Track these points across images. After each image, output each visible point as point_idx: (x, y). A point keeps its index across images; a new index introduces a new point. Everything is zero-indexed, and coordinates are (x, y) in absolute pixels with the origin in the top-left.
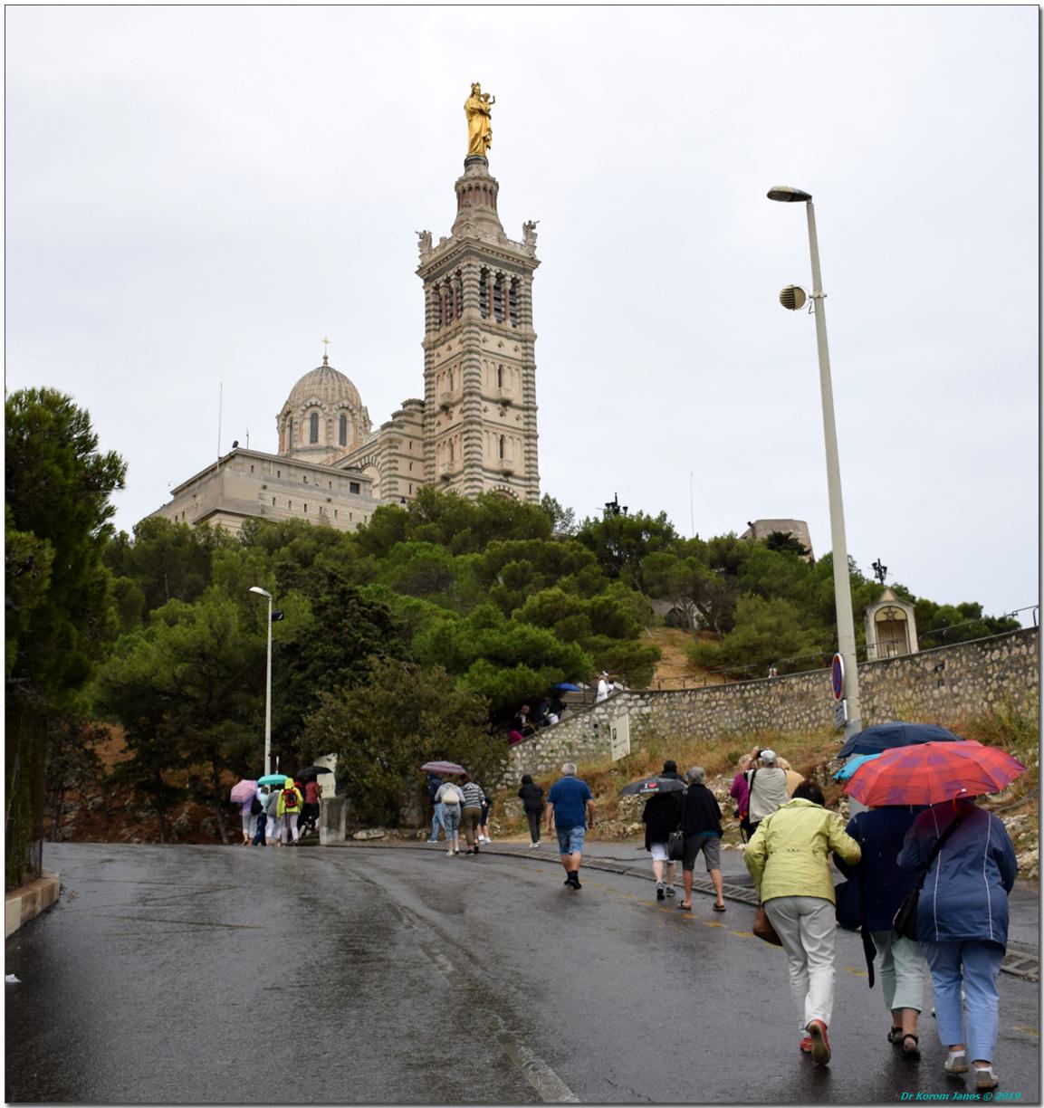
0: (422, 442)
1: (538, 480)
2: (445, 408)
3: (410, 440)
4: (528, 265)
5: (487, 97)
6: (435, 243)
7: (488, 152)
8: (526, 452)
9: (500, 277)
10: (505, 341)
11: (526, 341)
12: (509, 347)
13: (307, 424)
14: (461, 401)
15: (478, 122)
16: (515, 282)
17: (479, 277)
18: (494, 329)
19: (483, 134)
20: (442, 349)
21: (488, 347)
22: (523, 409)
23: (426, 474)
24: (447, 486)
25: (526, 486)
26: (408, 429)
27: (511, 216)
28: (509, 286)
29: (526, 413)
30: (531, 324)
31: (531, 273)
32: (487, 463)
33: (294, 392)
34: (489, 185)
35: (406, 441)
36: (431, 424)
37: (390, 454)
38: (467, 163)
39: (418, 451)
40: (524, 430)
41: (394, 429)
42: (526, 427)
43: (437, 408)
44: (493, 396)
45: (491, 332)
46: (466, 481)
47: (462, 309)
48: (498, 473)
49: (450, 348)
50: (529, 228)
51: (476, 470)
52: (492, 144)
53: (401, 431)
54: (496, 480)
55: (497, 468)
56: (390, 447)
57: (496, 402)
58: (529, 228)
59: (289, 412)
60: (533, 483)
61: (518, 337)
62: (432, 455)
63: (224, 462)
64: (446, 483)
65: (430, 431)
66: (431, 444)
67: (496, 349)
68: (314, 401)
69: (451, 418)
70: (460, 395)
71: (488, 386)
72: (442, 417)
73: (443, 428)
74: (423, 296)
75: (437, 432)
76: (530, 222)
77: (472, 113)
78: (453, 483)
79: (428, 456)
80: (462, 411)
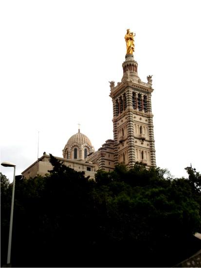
2: (121, 142)
3: (108, 154)
4: (148, 91)
5: (132, 34)
6: (116, 85)
7: (133, 53)
9: (140, 95)
10: (142, 118)
11: (149, 117)
12: (144, 120)
13: (73, 153)
14: (127, 139)
15: (130, 42)
16: (145, 97)
17: (132, 95)
18: (138, 113)
19: (132, 46)
20: (119, 122)
21: (136, 119)
26: (108, 150)
27: (142, 75)
28: (143, 98)
30: (151, 111)
31: (150, 93)
33: (68, 142)
34: (134, 64)
36: (116, 148)
37: (102, 159)
38: (126, 57)
39: (112, 158)
41: (103, 150)
43: (118, 142)
45: (137, 114)
47: (126, 107)
49: (122, 121)
50: (149, 78)
52: (135, 50)
56: (102, 157)
57: (139, 139)
58: (149, 78)
59: (67, 149)
63: (40, 160)
65: (117, 150)
66: (116, 155)
67: (139, 121)
68: (75, 144)
69: (123, 146)
70: (126, 137)
71: (136, 133)
72: (120, 146)
73: (121, 149)
74: (112, 103)
75: (119, 151)
77: (127, 39)
80: (127, 143)
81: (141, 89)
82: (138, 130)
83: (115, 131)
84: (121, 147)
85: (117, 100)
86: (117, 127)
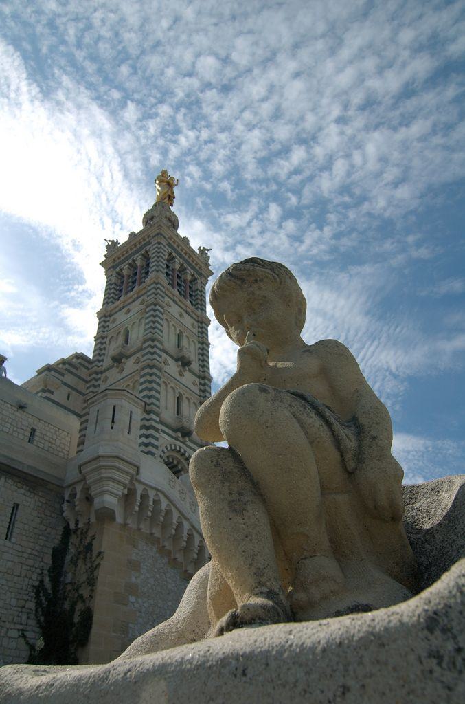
0: (82, 397)
2: (118, 360)
3: (68, 390)
9: (182, 270)
10: (185, 314)
12: (188, 321)
19: (170, 193)
21: (170, 310)
22: (199, 377)
26: (69, 379)
29: (202, 381)
35: (66, 390)
36: (96, 380)
41: (53, 373)
42: (202, 394)
43: (107, 362)
44: (173, 353)
48: (175, 431)
53: (61, 378)
54: (172, 437)
56: (44, 391)
57: (177, 360)
61: (195, 316)
65: (94, 386)
70: (139, 344)
73: (109, 382)
76: (204, 248)
81: (186, 257)
82: (174, 339)
83: (101, 339)
84: (113, 375)
85: (120, 274)
86: (111, 326)
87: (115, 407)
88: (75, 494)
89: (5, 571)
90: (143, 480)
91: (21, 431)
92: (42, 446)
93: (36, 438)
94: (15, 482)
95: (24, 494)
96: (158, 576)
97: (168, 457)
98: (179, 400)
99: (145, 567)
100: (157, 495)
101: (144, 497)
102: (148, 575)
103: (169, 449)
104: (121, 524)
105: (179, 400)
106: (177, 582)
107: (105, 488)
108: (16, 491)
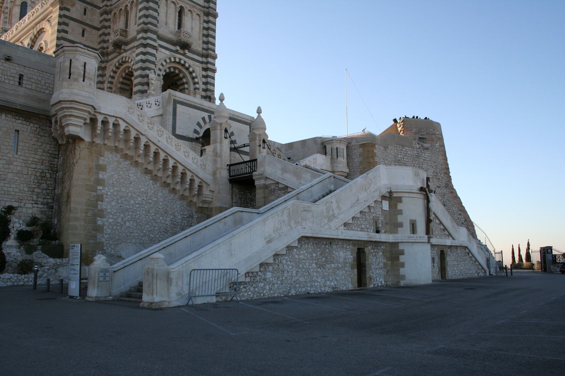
1: (215, 58)
8: (204, 28)
23: (99, 43)
24: (120, 54)
25: (202, 63)
32: (163, 30)
40: (204, 7)
46: (137, 47)
51: (149, 35)
55: (174, 38)
60: (210, 60)
62: (107, 24)
64: (118, 50)
66: (107, 13)
78: (125, 51)
79: (102, 24)
87: (71, 60)
88: (57, 121)
89: (17, 172)
90: (102, 112)
91: (12, 78)
92: (30, 87)
93: (24, 82)
94: (13, 116)
95: (22, 124)
96: (121, 173)
97: (169, 68)
98: (181, 13)
99: (111, 168)
100: (116, 120)
101: (105, 123)
102: (112, 173)
103: (168, 61)
104: (89, 142)
105: (181, 13)
106: (138, 176)
107: (68, 122)
108: (15, 122)
